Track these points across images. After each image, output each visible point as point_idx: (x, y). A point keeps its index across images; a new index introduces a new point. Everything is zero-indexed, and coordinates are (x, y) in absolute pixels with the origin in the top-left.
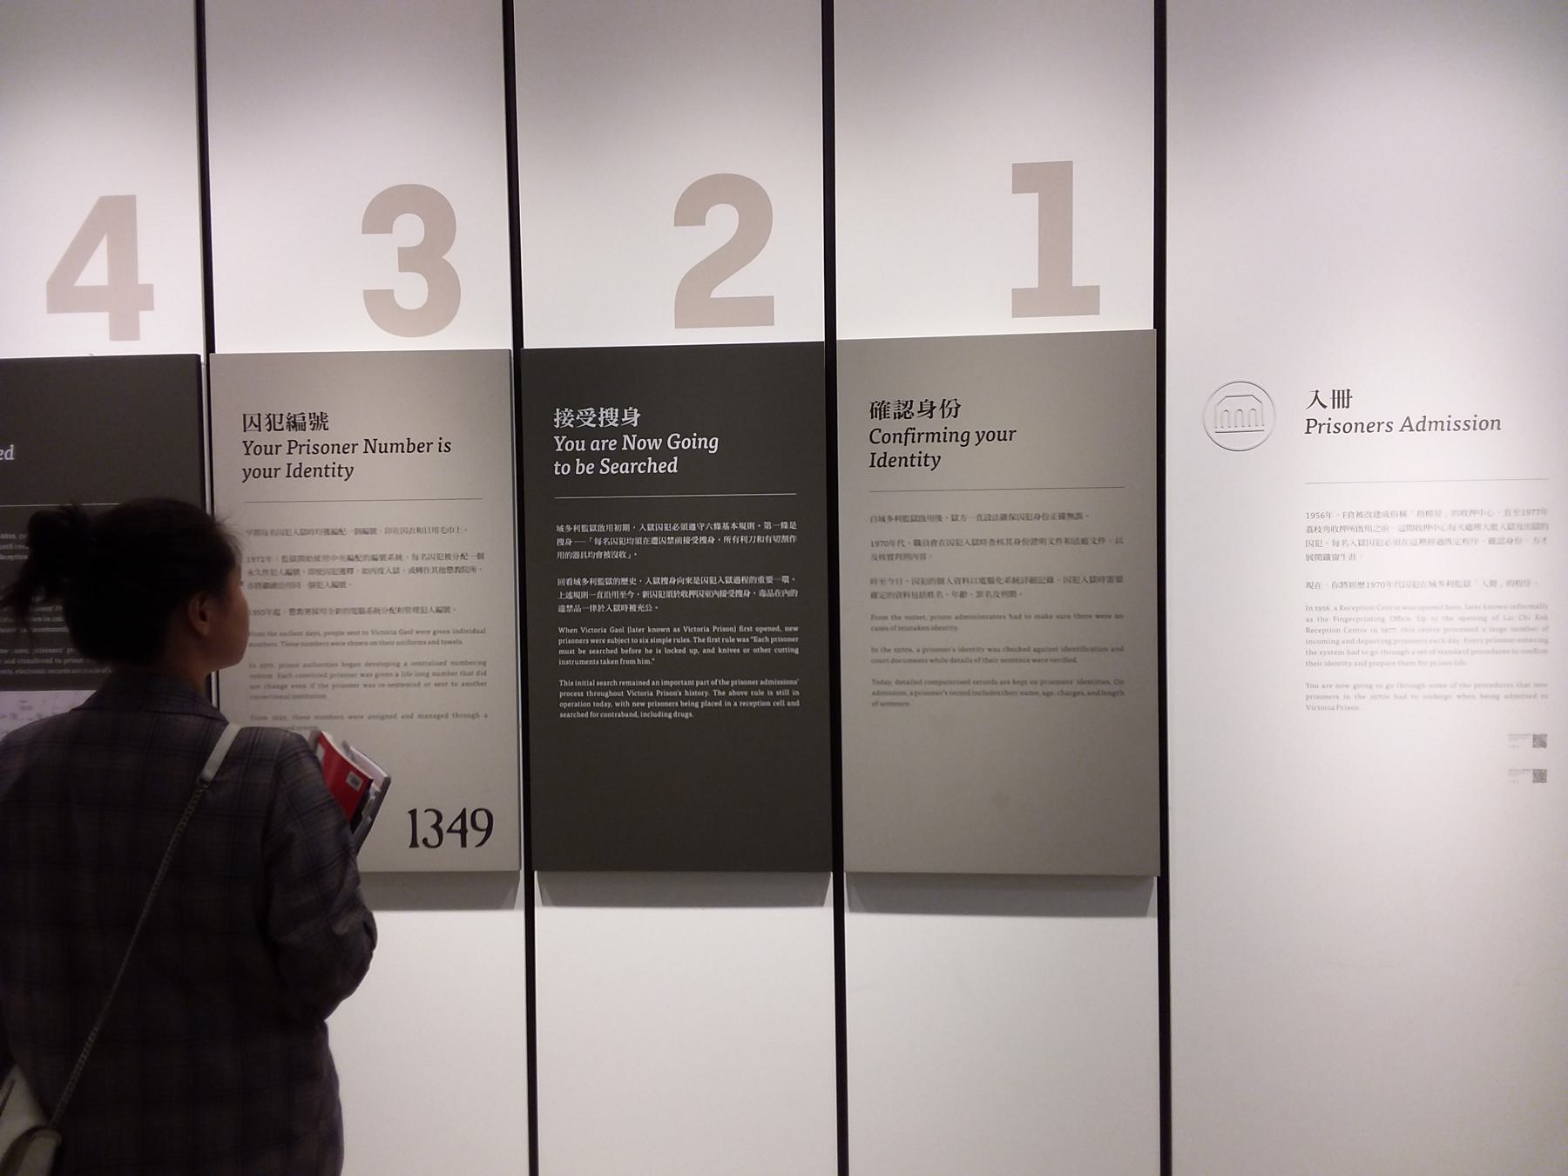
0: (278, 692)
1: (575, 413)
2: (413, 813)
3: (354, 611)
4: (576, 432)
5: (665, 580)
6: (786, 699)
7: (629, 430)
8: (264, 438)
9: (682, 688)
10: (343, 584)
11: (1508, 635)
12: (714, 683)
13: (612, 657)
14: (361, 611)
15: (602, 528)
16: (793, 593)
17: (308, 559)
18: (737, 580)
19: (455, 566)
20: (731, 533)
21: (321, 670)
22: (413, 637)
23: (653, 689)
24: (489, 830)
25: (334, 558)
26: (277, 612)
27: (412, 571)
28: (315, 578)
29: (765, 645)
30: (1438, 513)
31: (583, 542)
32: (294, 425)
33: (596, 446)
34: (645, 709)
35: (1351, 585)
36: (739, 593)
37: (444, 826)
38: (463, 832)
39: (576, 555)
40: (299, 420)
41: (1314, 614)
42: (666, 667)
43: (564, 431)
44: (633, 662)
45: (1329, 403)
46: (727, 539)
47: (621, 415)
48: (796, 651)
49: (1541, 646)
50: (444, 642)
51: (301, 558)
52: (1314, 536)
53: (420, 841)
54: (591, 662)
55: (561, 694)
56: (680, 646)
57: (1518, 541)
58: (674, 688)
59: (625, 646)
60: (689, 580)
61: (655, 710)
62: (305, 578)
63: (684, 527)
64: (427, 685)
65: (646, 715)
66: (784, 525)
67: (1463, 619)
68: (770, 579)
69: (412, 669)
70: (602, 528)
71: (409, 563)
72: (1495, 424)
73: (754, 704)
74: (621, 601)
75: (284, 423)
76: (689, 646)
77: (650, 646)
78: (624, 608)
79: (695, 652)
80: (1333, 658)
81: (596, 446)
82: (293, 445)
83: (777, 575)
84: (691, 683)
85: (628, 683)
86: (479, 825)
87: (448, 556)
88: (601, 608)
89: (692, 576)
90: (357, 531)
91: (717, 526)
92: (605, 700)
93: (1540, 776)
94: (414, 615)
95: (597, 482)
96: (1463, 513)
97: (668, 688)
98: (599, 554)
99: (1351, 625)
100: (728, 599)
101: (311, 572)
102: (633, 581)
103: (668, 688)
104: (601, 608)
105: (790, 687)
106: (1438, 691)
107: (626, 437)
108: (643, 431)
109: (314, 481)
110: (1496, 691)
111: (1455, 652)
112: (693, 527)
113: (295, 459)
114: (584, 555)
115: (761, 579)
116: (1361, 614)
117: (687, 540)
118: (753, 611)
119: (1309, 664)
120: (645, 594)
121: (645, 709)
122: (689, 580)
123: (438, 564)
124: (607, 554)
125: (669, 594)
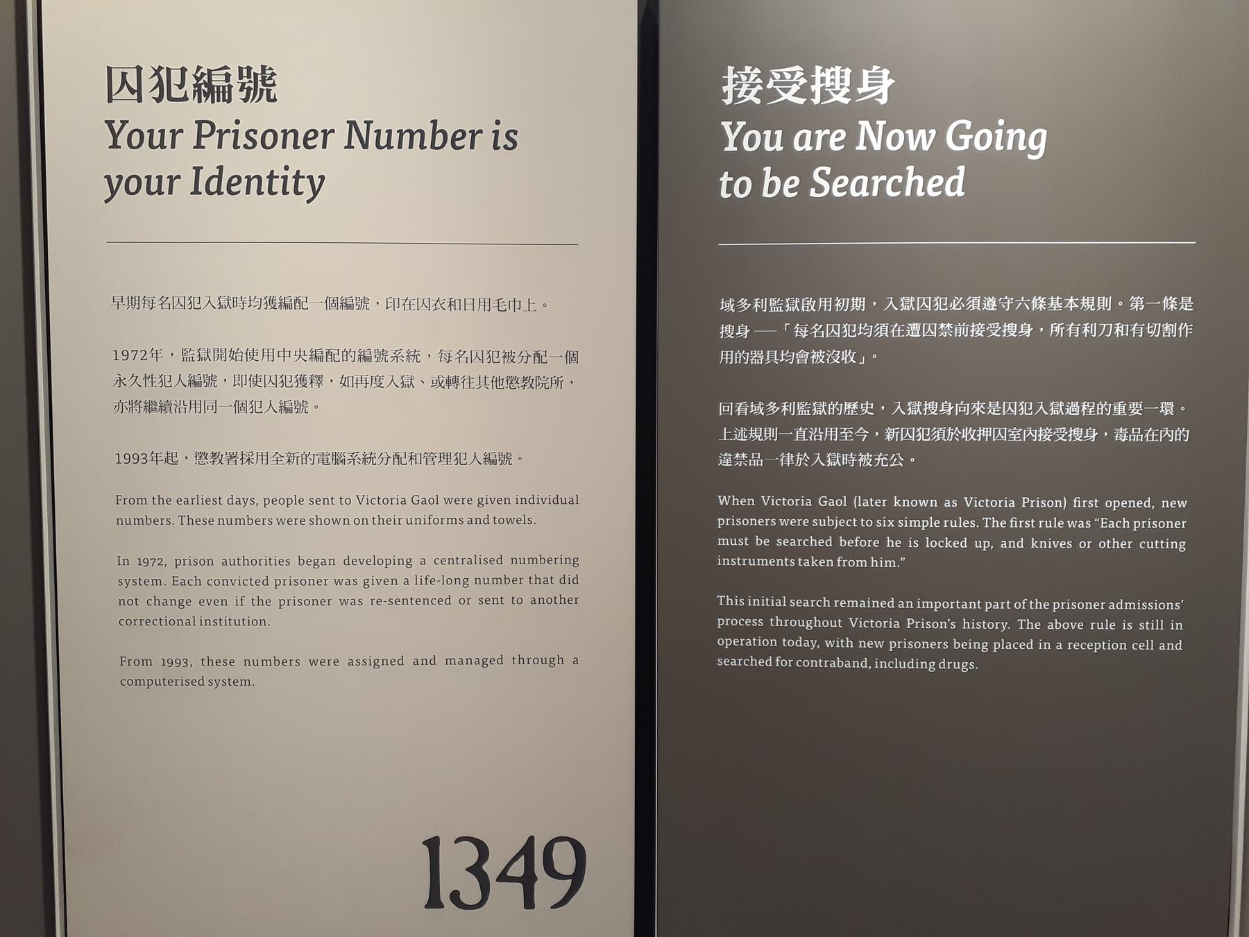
0: (173, 612)
1: (765, 77)
2: (433, 845)
3: (323, 459)
4: (757, 117)
5: (931, 407)
6: (1158, 637)
7: (871, 110)
8: (150, 114)
9: (957, 615)
10: (302, 406)
12: (1021, 605)
13: (820, 553)
14: (338, 459)
15: (809, 305)
16: (1179, 435)
17: (233, 355)
18: (1074, 409)
19: (521, 374)
20: (1065, 316)
21: (259, 572)
22: (441, 511)
23: (901, 615)
24: (577, 878)
25: (284, 354)
26: (171, 459)
27: (438, 383)
28: (247, 394)
29: (1121, 535)
31: (770, 331)
32: (208, 89)
33: (804, 141)
34: (884, 654)
36: (1076, 433)
37: (492, 868)
38: (528, 880)
39: (757, 357)
40: (218, 80)
42: (924, 574)
43: (739, 111)
44: (861, 563)
46: (1057, 329)
47: (856, 81)
48: (1182, 547)
50: (499, 521)
51: (220, 354)
53: (445, 897)
54: (781, 562)
55: (721, 622)
56: (956, 534)
58: (942, 615)
59: (848, 533)
60: (978, 408)
61: (904, 655)
62: (226, 393)
63: (974, 303)
64: (464, 601)
65: (884, 665)
66: (1170, 303)
68: (1136, 408)
69: (435, 572)
70: (809, 305)
71: (431, 368)
73: (1097, 647)
74: (841, 447)
75: (189, 87)
76: (972, 535)
77: (895, 533)
78: (848, 459)
79: (984, 545)
81: (804, 141)
82: (205, 131)
83: (1151, 400)
84: (975, 605)
85: (852, 603)
86: (558, 868)
87: (508, 356)
88: (801, 459)
89: (985, 400)
90: (330, 303)
91: (1038, 303)
92: (807, 635)
94: (441, 467)
95: (807, 214)
97: (929, 615)
98: (802, 356)
100: (1054, 445)
101: (239, 380)
102: (867, 408)
103: (929, 615)
104: (801, 459)
105: (1167, 616)
107: (865, 125)
108: (899, 113)
109: (245, 203)
112: (991, 304)
113: (210, 158)
114: (773, 357)
115: (1119, 408)
117: (977, 330)
118: (1097, 469)
120: (890, 434)
121: (884, 654)
122: (978, 408)
123: (492, 370)
124: (817, 356)
125: (939, 434)
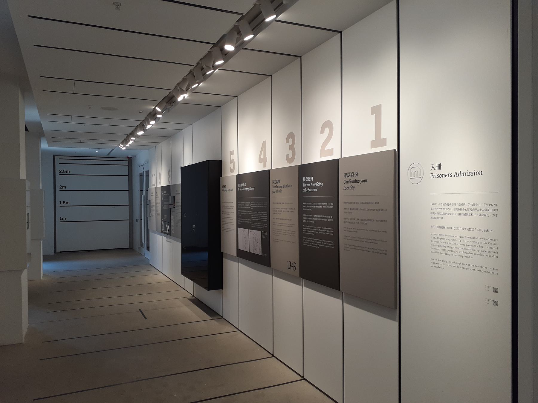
11: (485, 249)
30: (464, 205)
35: (442, 227)
41: (433, 236)
45: (436, 168)
49: (495, 255)
52: (433, 211)
57: (488, 215)
67: (472, 242)
72: (481, 173)
80: (438, 251)
93: (496, 303)
96: (471, 205)
99: (442, 241)
106: (465, 266)
110: (481, 269)
111: (469, 253)
116: (444, 237)
119: (432, 252)
